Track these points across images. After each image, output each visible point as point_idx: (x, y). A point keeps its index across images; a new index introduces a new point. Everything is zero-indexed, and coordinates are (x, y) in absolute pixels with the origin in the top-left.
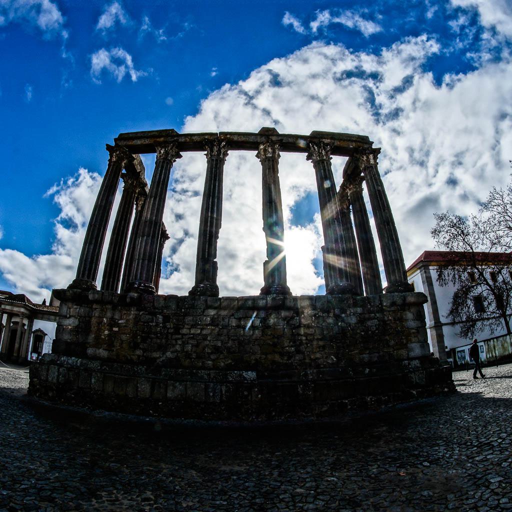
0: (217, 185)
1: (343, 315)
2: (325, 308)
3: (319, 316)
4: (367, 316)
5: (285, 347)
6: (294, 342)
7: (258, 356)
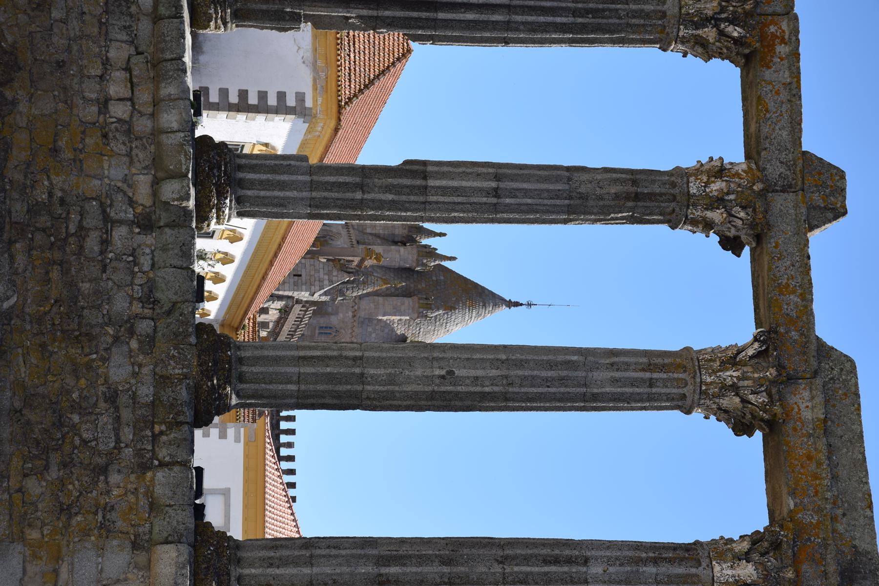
0: (558, 20)
1: (134, 344)
2: (158, 295)
3: (133, 274)
4: (126, 415)
5: (49, 178)
6: (62, 201)
7: (23, 107)
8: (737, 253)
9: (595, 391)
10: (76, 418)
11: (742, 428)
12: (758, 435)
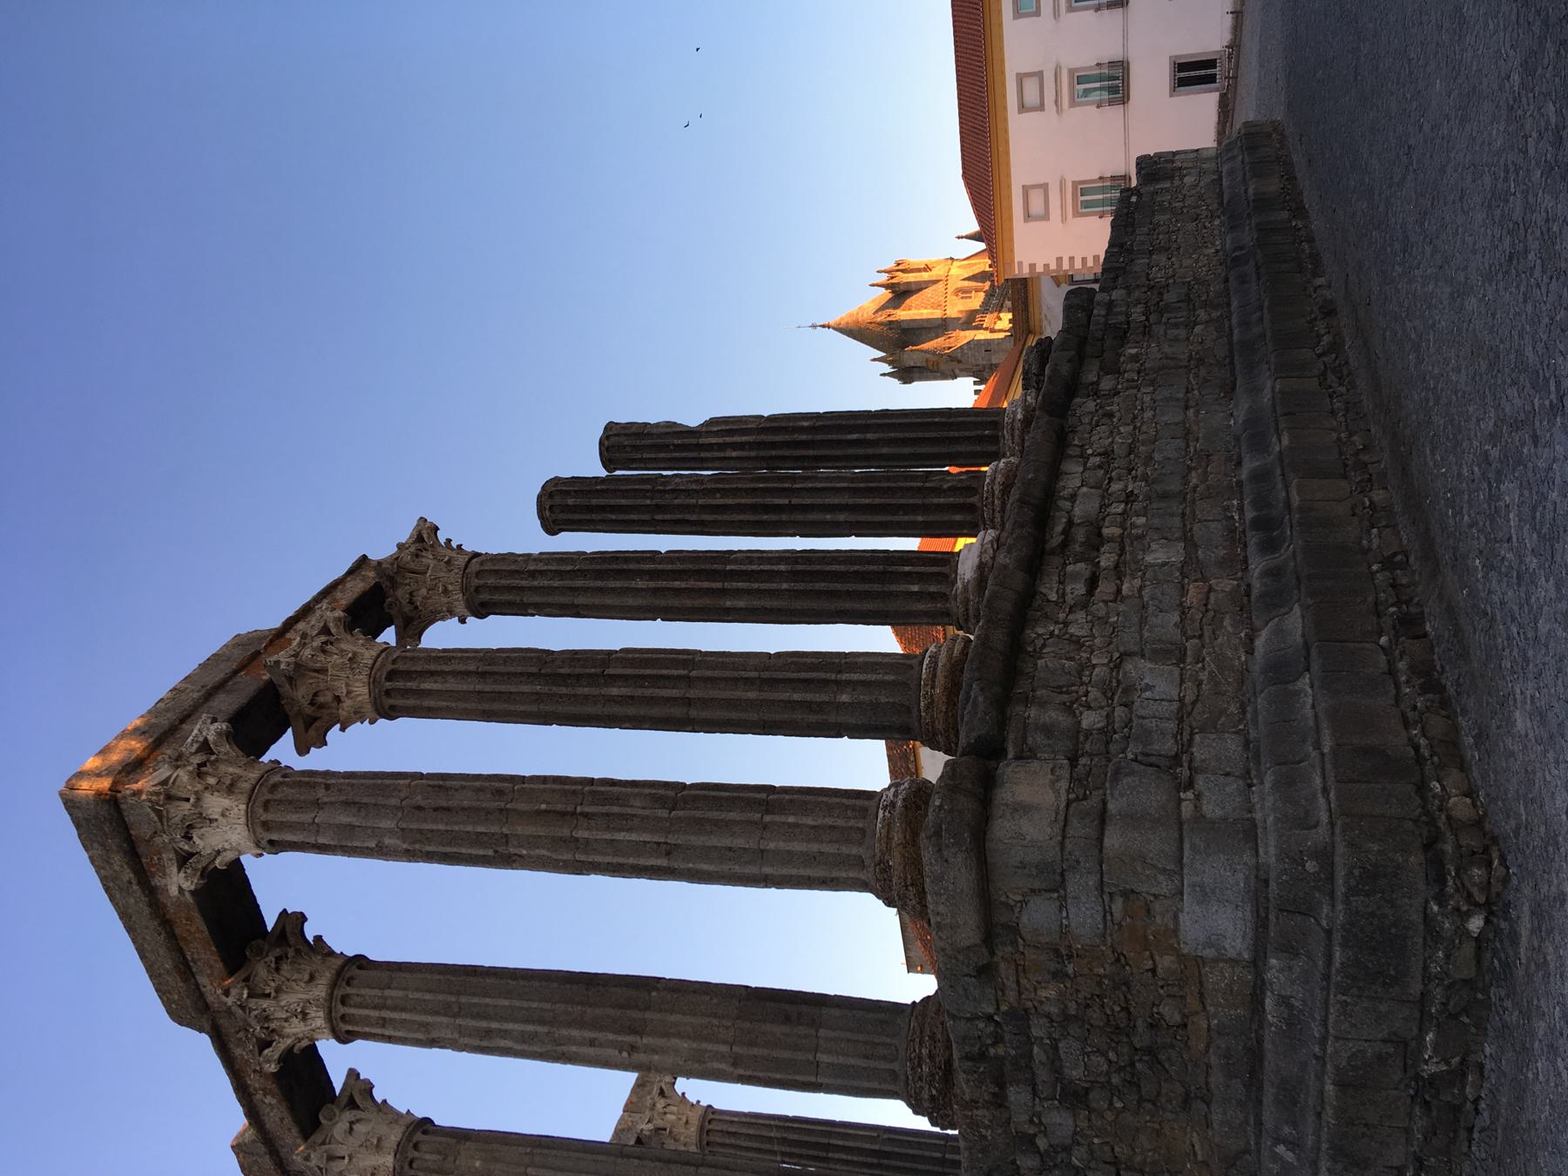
1: (1042, 1143)
8: (353, 1074)
9: (445, 1020)
10: (1115, 1080)
11: (293, 922)
12: (270, 922)
